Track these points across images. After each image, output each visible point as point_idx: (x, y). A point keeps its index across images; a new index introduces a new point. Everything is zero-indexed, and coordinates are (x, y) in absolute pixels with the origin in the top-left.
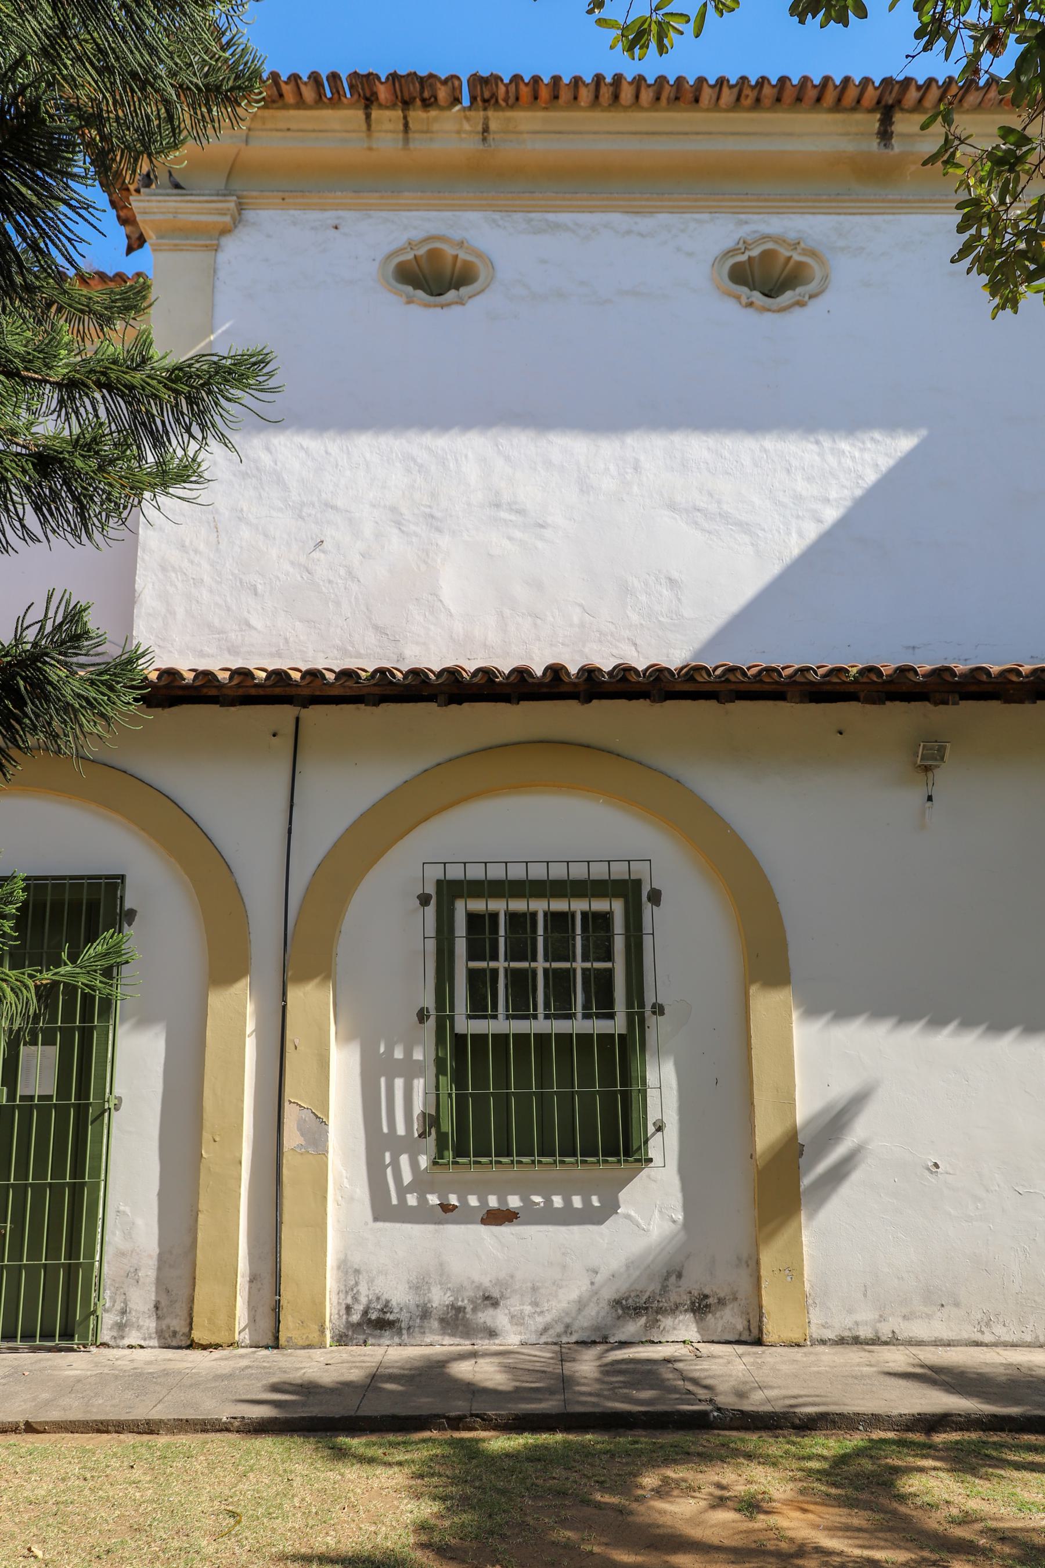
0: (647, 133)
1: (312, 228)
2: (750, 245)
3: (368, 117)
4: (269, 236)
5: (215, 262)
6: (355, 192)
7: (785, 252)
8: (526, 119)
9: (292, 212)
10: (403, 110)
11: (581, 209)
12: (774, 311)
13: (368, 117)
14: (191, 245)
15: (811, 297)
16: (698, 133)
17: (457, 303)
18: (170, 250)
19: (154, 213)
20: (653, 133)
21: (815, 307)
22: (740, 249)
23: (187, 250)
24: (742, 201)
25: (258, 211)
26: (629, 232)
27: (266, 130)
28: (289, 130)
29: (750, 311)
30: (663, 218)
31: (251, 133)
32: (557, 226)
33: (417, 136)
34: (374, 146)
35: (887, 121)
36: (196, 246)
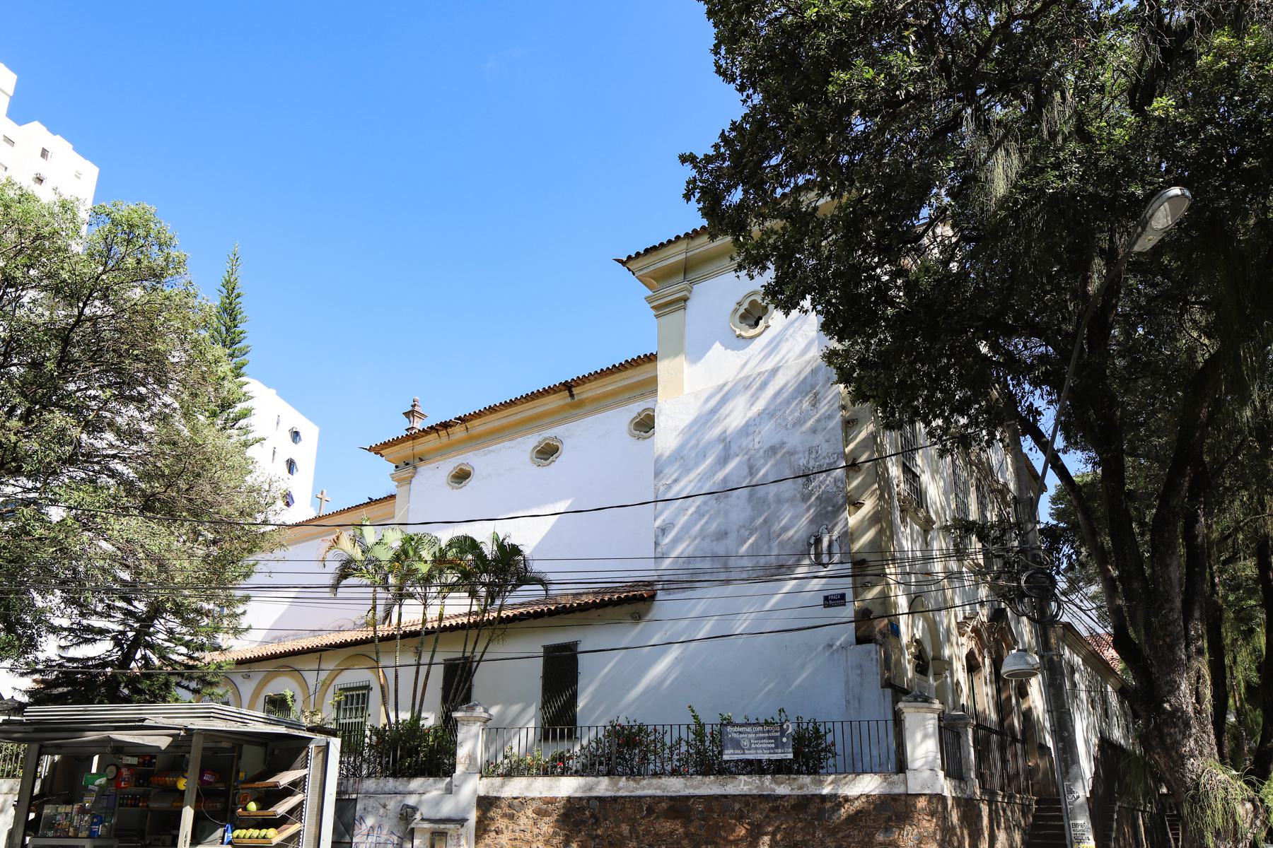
8: (476, 422)
35: (570, 392)
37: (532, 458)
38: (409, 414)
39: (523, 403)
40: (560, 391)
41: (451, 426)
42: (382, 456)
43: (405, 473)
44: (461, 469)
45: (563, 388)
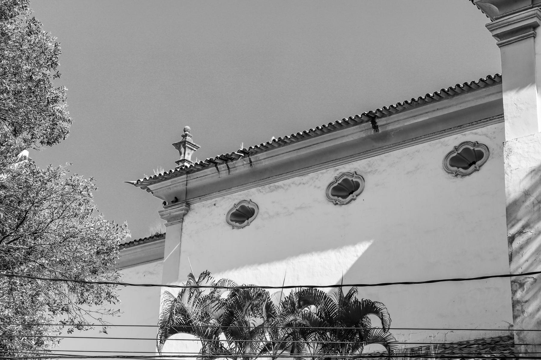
0: (298, 149)
1: (208, 207)
2: (338, 179)
3: (217, 168)
4: (197, 213)
5: (182, 226)
6: (219, 191)
7: (350, 179)
8: (261, 155)
9: (203, 202)
10: (226, 164)
11: (285, 179)
12: (345, 204)
13: (217, 168)
14: (175, 222)
15: (357, 196)
16: (314, 145)
17: (247, 225)
18: (170, 225)
19: (165, 215)
20: (300, 149)
21: (359, 199)
22: (334, 182)
23: (175, 224)
24: (335, 162)
25: (195, 204)
26: (300, 184)
27: (191, 179)
28: (197, 177)
29: (337, 206)
30: (311, 175)
31: (187, 182)
32: (278, 187)
33: (232, 169)
34: (220, 176)
36: (177, 222)
37: (327, 195)
38: (181, 145)
39: (317, 135)
40: (362, 122)
41: (232, 159)
42: (149, 190)
43: (176, 210)
44: (243, 207)
45: (365, 119)
